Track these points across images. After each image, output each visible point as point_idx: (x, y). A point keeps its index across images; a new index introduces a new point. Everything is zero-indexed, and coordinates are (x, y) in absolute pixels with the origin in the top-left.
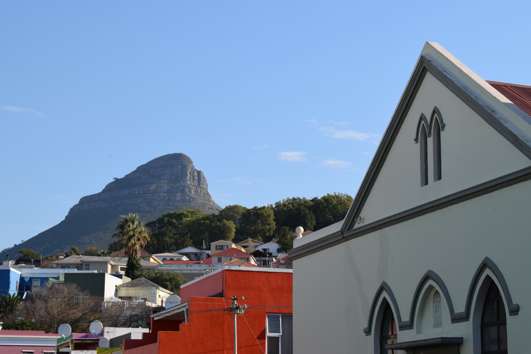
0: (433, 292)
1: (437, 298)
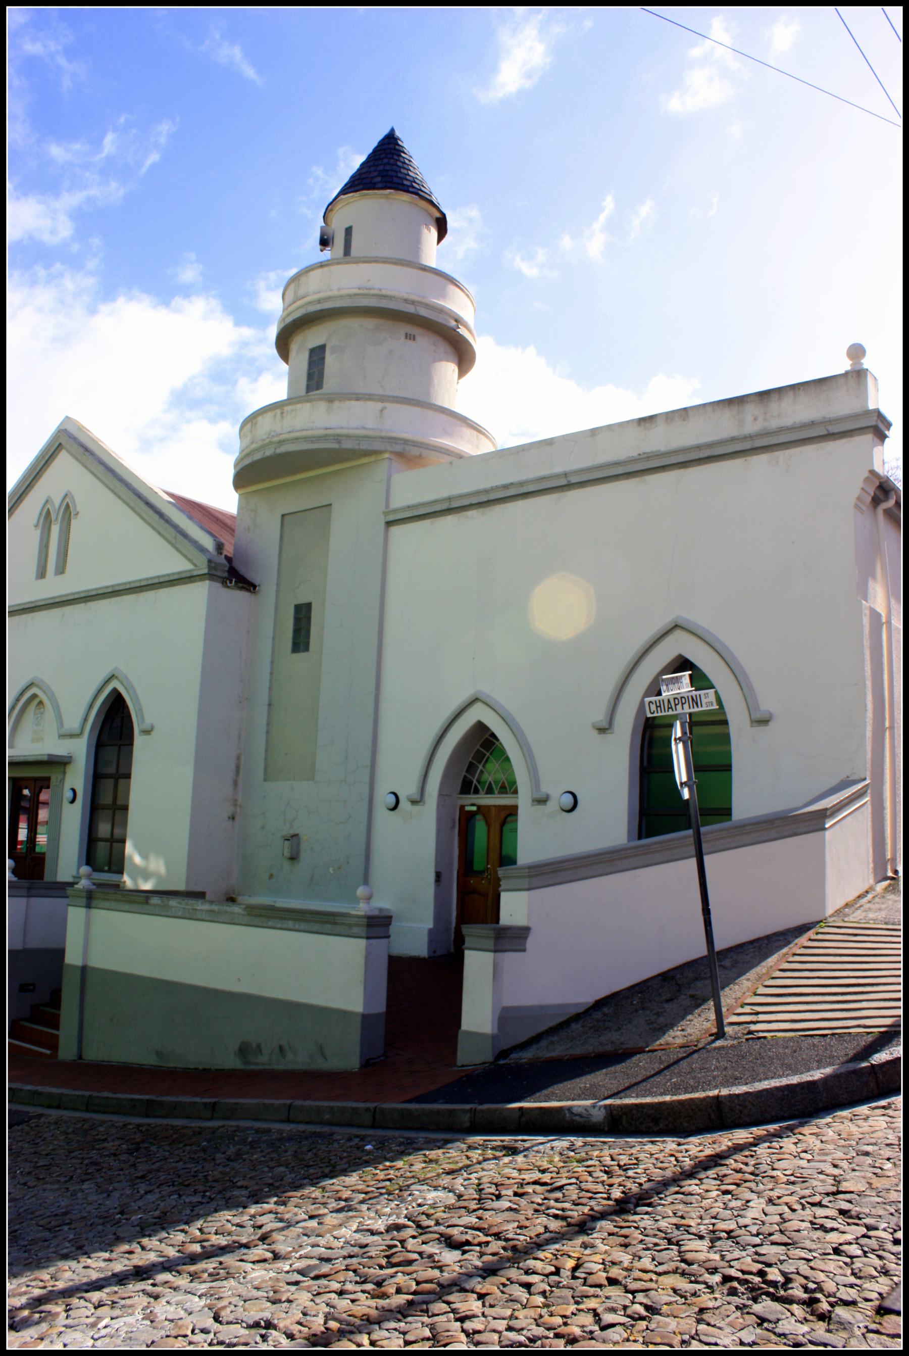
0: (36, 701)
1: (40, 709)
